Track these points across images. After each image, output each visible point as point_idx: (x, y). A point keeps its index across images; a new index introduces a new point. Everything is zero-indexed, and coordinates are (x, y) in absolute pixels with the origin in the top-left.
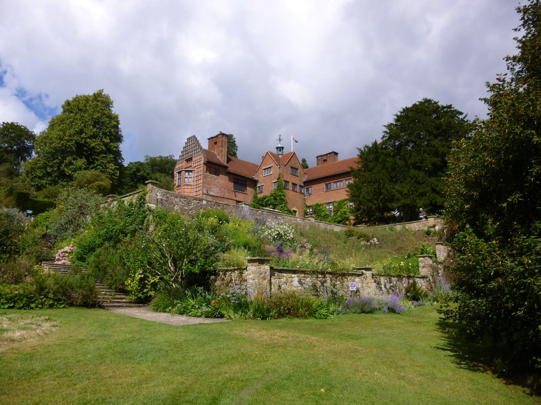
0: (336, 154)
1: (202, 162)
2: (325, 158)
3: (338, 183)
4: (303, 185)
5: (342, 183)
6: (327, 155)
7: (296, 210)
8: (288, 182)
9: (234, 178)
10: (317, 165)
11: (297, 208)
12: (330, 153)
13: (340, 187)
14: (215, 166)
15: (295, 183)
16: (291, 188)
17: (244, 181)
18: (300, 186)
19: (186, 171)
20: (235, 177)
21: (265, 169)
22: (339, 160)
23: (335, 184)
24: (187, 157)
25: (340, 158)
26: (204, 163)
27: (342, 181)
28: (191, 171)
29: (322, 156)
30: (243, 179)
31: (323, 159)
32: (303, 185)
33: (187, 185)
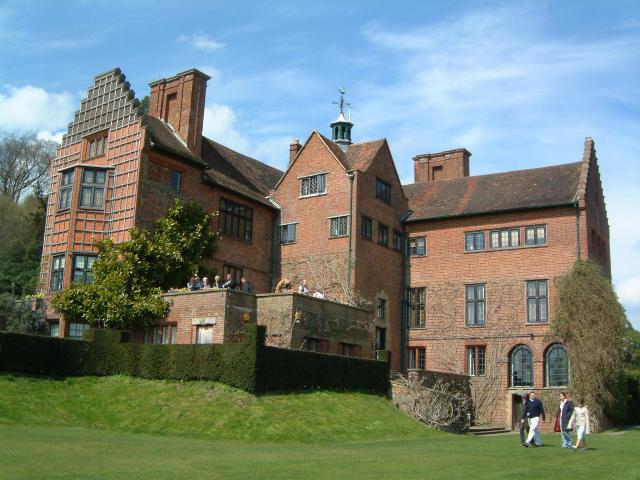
0: (466, 154)
1: (140, 145)
2: (435, 162)
3: (505, 235)
4: (400, 229)
5: (515, 234)
6: (444, 154)
7: (386, 297)
8: (370, 220)
9: (222, 198)
10: (416, 179)
11: (387, 292)
12: (452, 152)
13: (510, 244)
14: (174, 162)
15: (384, 222)
16: (376, 237)
17: (247, 208)
18: (395, 232)
19: (87, 169)
20: (227, 196)
21: (304, 180)
22: (471, 175)
23: (495, 236)
24: (92, 128)
26: (144, 151)
27: (516, 228)
28: (104, 170)
29: (429, 157)
30: (243, 202)
31: (430, 165)
32: (400, 229)
33: (86, 211)
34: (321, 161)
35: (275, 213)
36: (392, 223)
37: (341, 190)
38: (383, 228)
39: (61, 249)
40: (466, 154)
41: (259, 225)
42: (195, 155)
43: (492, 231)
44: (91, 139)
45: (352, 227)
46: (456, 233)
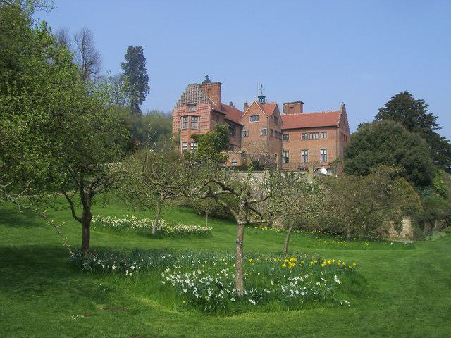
0: (302, 103)
1: (209, 110)
2: (291, 105)
25: (306, 110)
34: (258, 111)
35: (241, 127)
36: (279, 131)
37: (264, 121)
38: (276, 132)
39: (186, 141)
40: (302, 103)
41: (237, 131)
42: (219, 110)
43: (312, 133)
44: (189, 106)
45: (268, 133)
46: (299, 134)
